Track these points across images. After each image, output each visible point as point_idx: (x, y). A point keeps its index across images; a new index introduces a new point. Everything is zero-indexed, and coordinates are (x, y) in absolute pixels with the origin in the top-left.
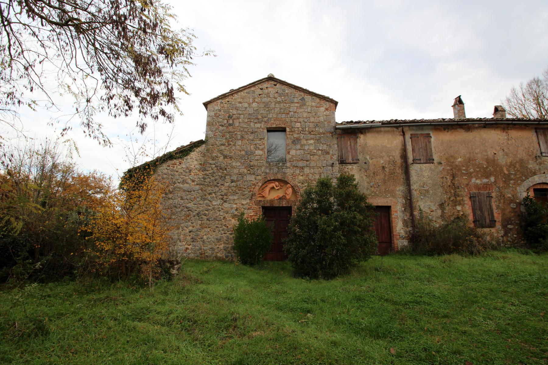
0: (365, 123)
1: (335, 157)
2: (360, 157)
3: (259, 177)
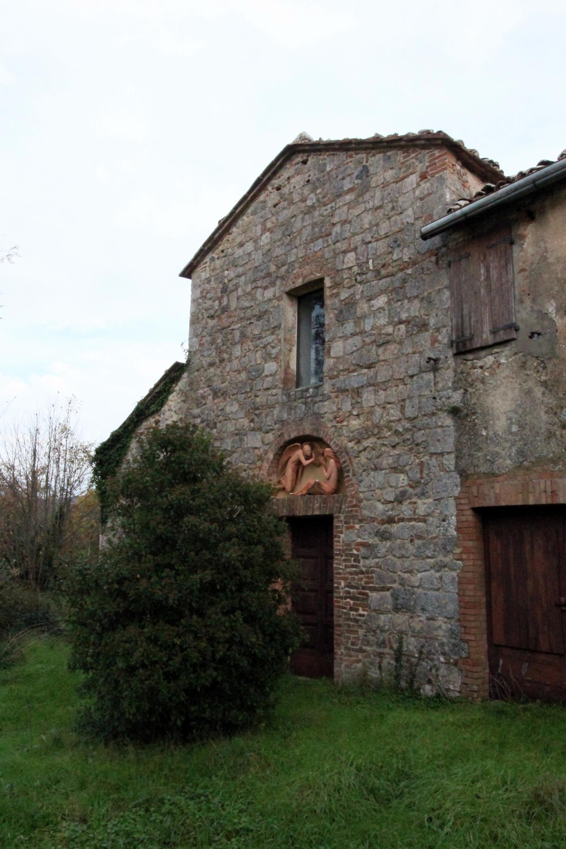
0: (531, 171)
1: (444, 338)
2: (523, 315)
3: (270, 437)
